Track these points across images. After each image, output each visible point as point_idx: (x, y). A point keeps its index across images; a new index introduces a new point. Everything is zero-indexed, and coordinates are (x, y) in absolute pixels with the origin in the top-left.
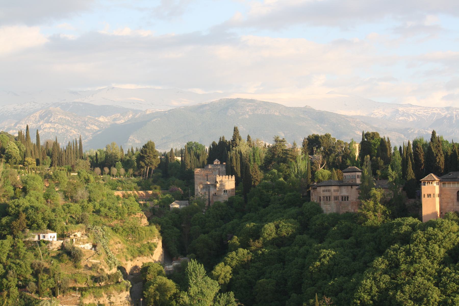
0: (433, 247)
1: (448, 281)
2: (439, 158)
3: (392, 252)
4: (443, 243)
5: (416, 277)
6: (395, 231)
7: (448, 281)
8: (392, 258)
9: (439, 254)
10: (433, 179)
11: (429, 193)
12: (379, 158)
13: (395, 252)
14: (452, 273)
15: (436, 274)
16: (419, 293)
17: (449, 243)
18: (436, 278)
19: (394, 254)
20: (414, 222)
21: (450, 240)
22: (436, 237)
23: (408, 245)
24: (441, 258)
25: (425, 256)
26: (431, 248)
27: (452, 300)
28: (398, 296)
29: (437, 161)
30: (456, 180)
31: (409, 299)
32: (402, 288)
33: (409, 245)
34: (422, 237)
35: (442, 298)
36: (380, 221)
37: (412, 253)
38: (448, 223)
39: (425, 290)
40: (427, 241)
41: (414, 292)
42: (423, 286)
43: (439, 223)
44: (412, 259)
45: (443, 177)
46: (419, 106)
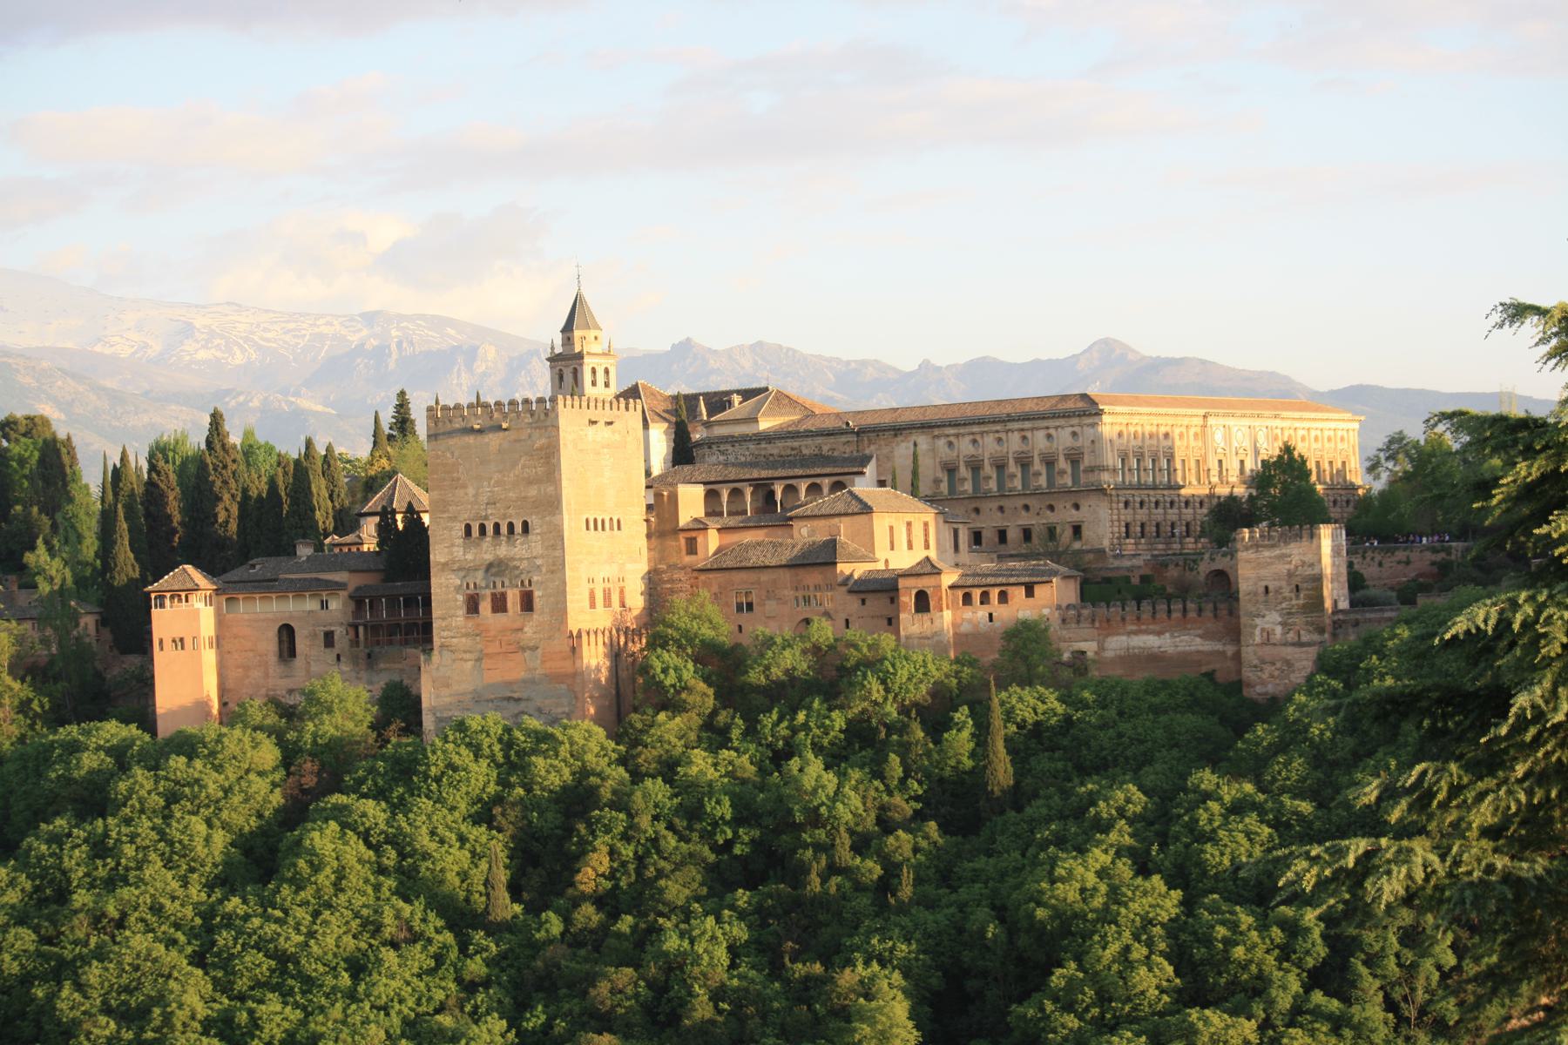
0: (186, 827)
1: (239, 947)
2: (227, 510)
3: (44, 847)
4: (220, 810)
5: (128, 933)
6: (55, 770)
7: (239, 947)
8: (46, 869)
9: (206, 851)
10: (190, 586)
11: (177, 636)
15: (198, 921)
16: (136, 989)
18: (196, 937)
19: (51, 855)
20: (124, 740)
21: (246, 801)
22: (196, 788)
23: (100, 820)
24: (215, 865)
25: (158, 859)
26: (177, 830)
27: (251, 1012)
28: (63, 1000)
29: (220, 520)
30: (273, 587)
32: (76, 973)
33: (104, 819)
34: (149, 793)
35: (217, 1006)
36: (9, 737)
37: (114, 848)
38: (240, 740)
39: (156, 980)
40: (167, 806)
41: (120, 986)
42: (149, 964)
43: (207, 739)
44: (112, 869)
45: (230, 576)
46: (267, 311)
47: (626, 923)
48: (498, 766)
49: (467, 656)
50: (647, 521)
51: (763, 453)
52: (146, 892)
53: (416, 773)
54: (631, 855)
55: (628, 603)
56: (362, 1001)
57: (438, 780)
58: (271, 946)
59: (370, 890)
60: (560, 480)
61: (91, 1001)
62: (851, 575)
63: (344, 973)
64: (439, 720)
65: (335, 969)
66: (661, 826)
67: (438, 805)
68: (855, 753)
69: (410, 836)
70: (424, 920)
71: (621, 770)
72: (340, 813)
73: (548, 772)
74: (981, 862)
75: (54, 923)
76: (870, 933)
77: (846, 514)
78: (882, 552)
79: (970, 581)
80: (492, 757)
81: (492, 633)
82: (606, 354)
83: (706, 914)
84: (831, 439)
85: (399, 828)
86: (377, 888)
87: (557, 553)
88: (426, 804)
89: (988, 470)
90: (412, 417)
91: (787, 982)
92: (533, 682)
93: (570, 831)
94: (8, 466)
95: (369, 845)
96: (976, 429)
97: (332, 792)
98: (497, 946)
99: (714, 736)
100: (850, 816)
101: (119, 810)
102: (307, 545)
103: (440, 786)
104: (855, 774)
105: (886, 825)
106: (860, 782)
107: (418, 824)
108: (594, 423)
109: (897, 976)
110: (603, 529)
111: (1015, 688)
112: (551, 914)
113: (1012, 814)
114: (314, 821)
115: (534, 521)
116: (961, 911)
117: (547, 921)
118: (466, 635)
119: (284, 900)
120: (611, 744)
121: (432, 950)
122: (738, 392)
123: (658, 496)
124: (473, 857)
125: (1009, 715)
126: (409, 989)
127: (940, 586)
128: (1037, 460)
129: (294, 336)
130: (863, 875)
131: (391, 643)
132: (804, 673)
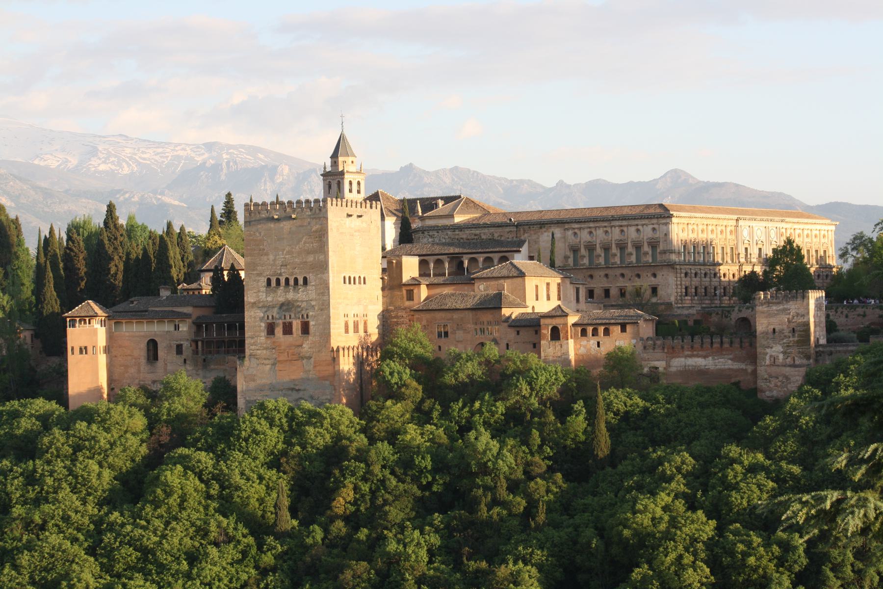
0: (85, 467)
1: (117, 543)
2: (116, 266)
4: (108, 456)
5: (47, 533)
6: (4, 429)
7: (117, 543)
9: (98, 482)
10: (91, 314)
11: (83, 345)
14: (125, 524)
15: (92, 527)
16: (52, 569)
17: (123, 456)
18: (91, 537)
20: (48, 410)
21: (124, 451)
22: (93, 443)
23: (31, 462)
24: (104, 491)
25: (68, 487)
26: (80, 468)
29: (112, 273)
30: (144, 315)
31: (29, 583)
32: (13, 559)
33: (34, 461)
34: (63, 445)
35: (103, 581)
38: (121, 412)
39: (64, 564)
40: (74, 453)
41: (41, 567)
42: (60, 553)
43: (101, 411)
44: (38, 493)
45: (116, 308)
46: (145, 141)
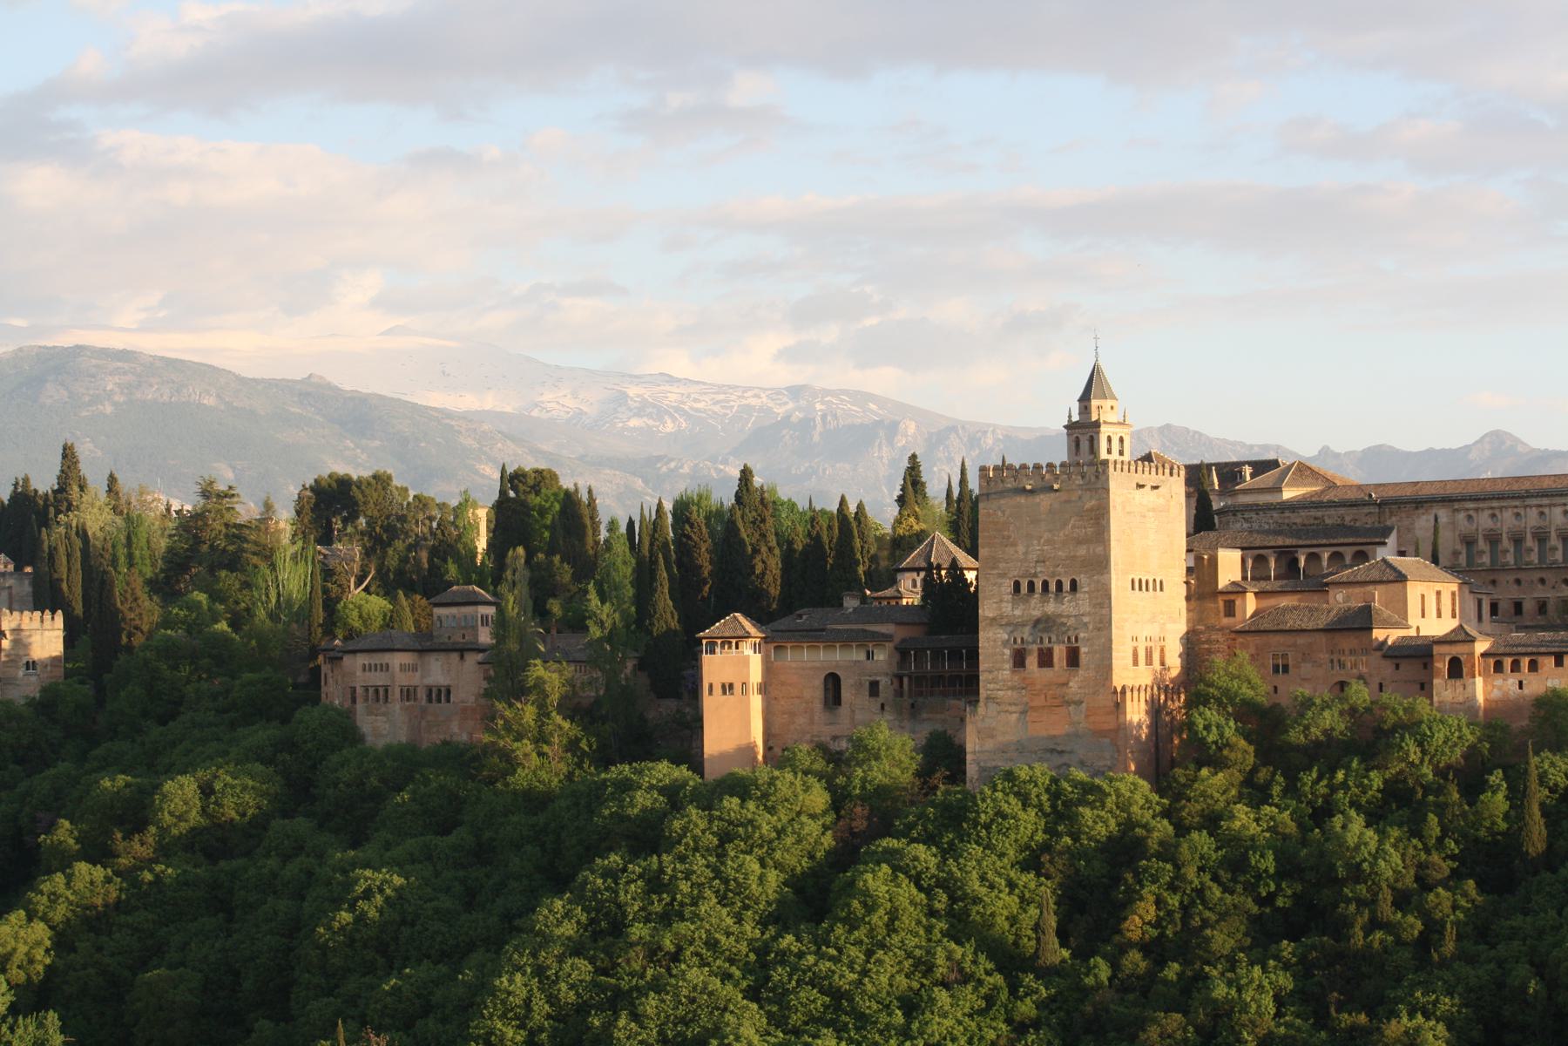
0: (740, 866)
1: (794, 982)
2: (764, 562)
3: (599, 881)
4: (774, 850)
5: (683, 966)
6: (610, 808)
7: (794, 982)
8: (602, 902)
9: (760, 889)
10: (740, 633)
11: (727, 680)
12: (557, 559)
13: (609, 880)
14: (805, 953)
15: (752, 957)
16: (692, 1020)
17: (796, 850)
18: (751, 972)
19: (606, 889)
20: (676, 780)
21: (799, 842)
22: (750, 829)
24: (769, 903)
25: (713, 896)
26: (732, 868)
28: (620, 1030)
29: (757, 572)
32: (633, 1004)
33: (659, 856)
34: (703, 832)
35: (773, 1040)
36: (557, 775)
37: (669, 884)
38: (792, 783)
39: (712, 1013)
40: (722, 844)
41: (676, 1017)
42: (705, 997)
43: (760, 782)
44: (667, 904)
47: (1172, 971)
48: (1046, 815)
49: (1013, 708)
50: (1187, 583)
51: (1286, 521)
52: (701, 927)
53: (966, 819)
54: (1177, 904)
55: (1168, 662)
56: (916, 1038)
57: (987, 827)
58: (826, 983)
59: (922, 932)
60: (1109, 540)
61: (648, 1031)
62: (1385, 641)
63: (897, 1011)
64: (982, 770)
65: (888, 1007)
66: (1206, 878)
67: (987, 851)
68: (1392, 812)
69: (961, 881)
70: (974, 962)
71: (1165, 822)
72: (890, 856)
73: (1095, 822)
74: (1517, 921)
75: (610, 955)
76: (1413, 986)
77: (1381, 582)
78: (1414, 619)
79: (1501, 650)
80: (1040, 806)
81: (1038, 687)
82: (1122, 424)
83: (1252, 964)
84: (1354, 510)
85: (950, 873)
86: (929, 929)
87: (1104, 611)
88: (976, 850)
89: (1506, 543)
90: (923, 480)
91: (1332, 1031)
92: (1077, 735)
93: (1117, 880)
94: (529, 516)
95: (920, 888)
96: (1495, 504)
97: (883, 836)
98: (1047, 989)
99: (1255, 793)
100: (1391, 873)
101: (673, 847)
102: (854, 597)
103: (989, 833)
104: (1395, 833)
105: (1424, 884)
106: (1399, 840)
107: (968, 869)
108: (1142, 486)
109: (1441, 1028)
110: (1147, 589)
111: (1546, 754)
112: (1099, 959)
113: (1547, 876)
114: (866, 863)
115: (1082, 579)
116: (1500, 967)
117: (1095, 966)
118: (1012, 688)
119: (838, 938)
120: (1155, 797)
121: (983, 991)
122: (1250, 463)
123: (1199, 559)
124: (1021, 902)
125: (1542, 778)
126: (961, 1028)
127: (1472, 654)
128: (1553, 535)
129: (723, 407)
130: (1404, 930)
131: (932, 694)
132: (1341, 733)
